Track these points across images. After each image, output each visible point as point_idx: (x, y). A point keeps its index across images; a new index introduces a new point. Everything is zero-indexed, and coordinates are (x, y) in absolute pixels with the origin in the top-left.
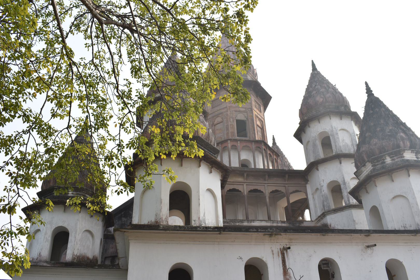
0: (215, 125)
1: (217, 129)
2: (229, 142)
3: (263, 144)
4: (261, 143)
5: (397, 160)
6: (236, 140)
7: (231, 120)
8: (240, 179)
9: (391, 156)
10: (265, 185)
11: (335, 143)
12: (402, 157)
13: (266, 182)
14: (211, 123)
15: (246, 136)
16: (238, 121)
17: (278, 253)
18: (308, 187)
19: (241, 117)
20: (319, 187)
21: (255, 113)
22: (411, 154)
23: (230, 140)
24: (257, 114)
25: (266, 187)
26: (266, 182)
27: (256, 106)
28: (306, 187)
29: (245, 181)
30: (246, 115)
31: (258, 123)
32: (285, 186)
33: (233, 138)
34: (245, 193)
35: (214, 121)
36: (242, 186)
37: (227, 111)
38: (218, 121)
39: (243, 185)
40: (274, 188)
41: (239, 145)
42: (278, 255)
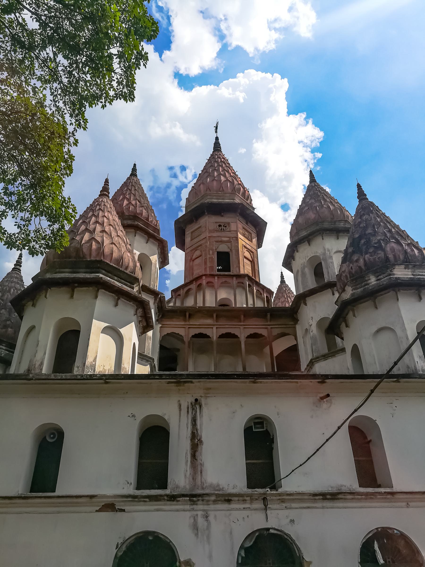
0: (193, 261)
1: (196, 265)
3: (247, 278)
5: (385, 280)
6: (213, 276)
7: (211, 252)
8: (209, 321)
9: (377, 274)
10: (241, 327)
11: (327, 269)
12: (390, 275)
13: (242, 324)
14: (190, 258)
15: (230, 272)
16: (219, 253)
17: (188, 408)
18: (298, 327)
19: (223, 248)
20: (307, 327)
21: (241, 243)
22: (404, 270)
23: (205, 275)
24: (244, 244)
26: (242, 324)
27: (244, 235)
28: (295, 328)
30: (230, 246)
31: (247, 254)
33: (212, 273)
34: (215, 338)
35: (193, 256)
36: (212, 329)
37: (206, 242)
39: (213, 328)
40: (252, 331)
41: (216, 280)
42: (188, 412)
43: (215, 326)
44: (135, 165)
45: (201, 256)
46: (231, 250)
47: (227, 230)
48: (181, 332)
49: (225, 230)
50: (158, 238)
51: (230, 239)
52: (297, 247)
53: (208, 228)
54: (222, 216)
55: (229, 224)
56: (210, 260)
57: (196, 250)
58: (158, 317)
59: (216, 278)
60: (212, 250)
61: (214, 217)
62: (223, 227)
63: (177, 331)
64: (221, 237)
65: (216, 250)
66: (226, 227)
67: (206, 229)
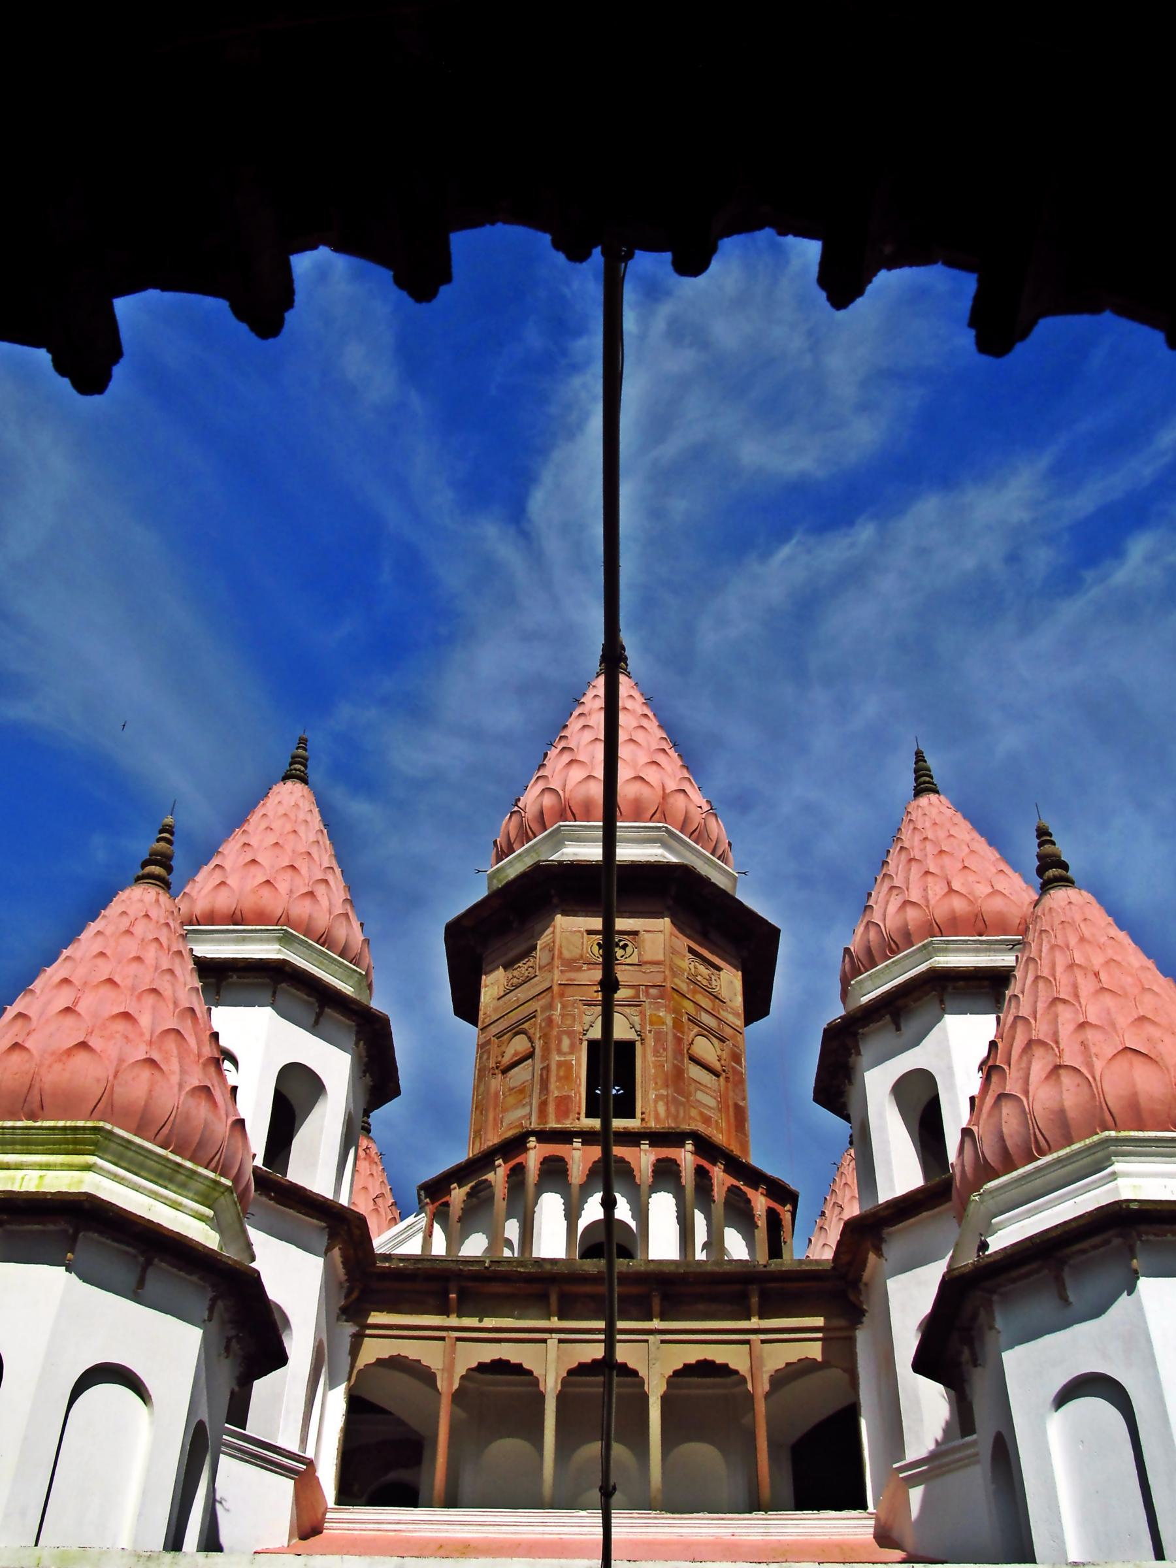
2: (532, 1142)
3: (689, 1146)
6: (565, 1137)
7: (566, 1042)
10: (650, 1338)
15: (631, 1115)
25: (652, 1348)
29: (555, 1322)
30: (637, 1020)
32: (747, 1342)
37: (550, 1006)
38: (516, 1054)
40: (694, 1354)
43: (554, 1335)
45: (530, 1055)
47: (628, 961)
48: (428, 1354)
49: (623, 960)
50: (354, 1007)
52: (859, 1036)
53: (561, 953)
55: (635, 933)
56: (562, 1073)
58: (347, 1296)
60: (571, 1034)
63: (411, 1350)
67: (553, 959)
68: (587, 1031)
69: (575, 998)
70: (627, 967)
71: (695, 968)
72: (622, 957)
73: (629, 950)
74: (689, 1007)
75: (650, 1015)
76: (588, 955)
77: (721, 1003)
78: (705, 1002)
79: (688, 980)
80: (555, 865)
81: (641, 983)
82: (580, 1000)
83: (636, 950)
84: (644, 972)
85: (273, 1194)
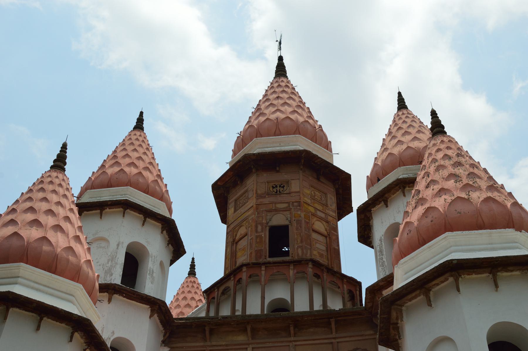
0: (236, 243)
1: (239, 249)
3: (310, 265)
4: (308, 264)
10: (291, 344)
19: (278, 220)
26: (292, 339)
32: (332, 343)
35: (236, 235)
38: (241, 235)
39: (247, 348)
41: (263, 272)
44: (141, 113)
46: (290, 222)
47: (285, 192)
50: (159, 217)
51: (289, 206)
52: (372, 212)
54: (278, 172)
56: (258, 240)
57: (241, 227)
58: (164, 336)
59: (263, 268)
60: (262, 224)
61: (265, 175)
62: (278, 188)
64: (276, 203)
65: (267, 224)
66: (283, 187)
68: (268, 222)
69: (263, 209)
70: (285, 195)
71: (314, 193)
72: (282, 191)
73: (285, 188)
74: (312, 210)
75: (295, 214)
76: (268, 191)
77: (326, 207)
78: (319, 207)
79: (311, 199)
80: (252, 155)
81: (291, 201)
82: (265, 210)
83: (288, 188)
84: (292, 196)
85: (124, 295)
